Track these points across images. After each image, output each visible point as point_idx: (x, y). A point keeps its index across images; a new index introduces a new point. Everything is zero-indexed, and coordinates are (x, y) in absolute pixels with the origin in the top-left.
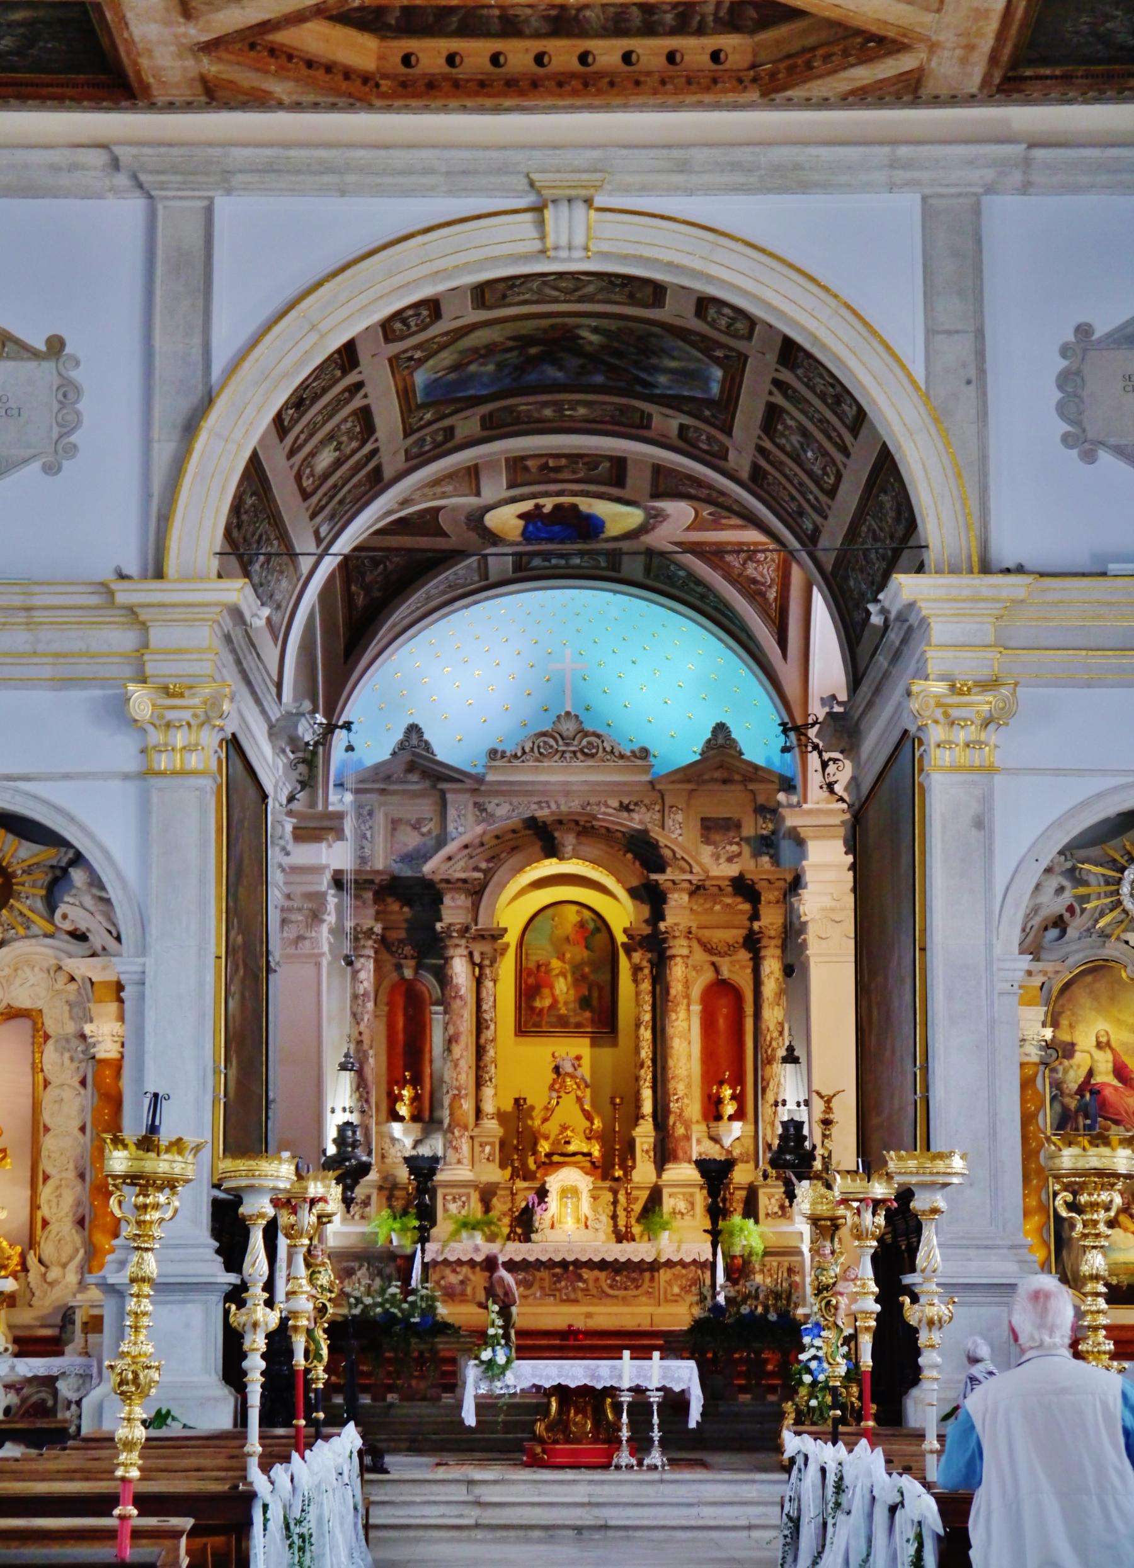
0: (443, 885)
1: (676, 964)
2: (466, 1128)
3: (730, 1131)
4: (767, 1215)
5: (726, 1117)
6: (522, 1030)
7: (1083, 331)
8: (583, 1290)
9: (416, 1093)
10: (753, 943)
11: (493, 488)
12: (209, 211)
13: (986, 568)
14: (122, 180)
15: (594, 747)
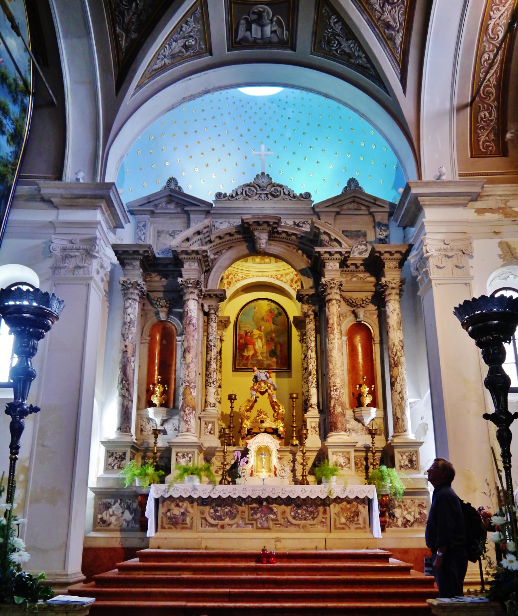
0: (184, 256)
1: (332, 305)
2: (194, 408)
3: (370, 413)
4: (401, 466)
5: (365, 405)
6: (236, 369)
8: (273, 520)
9: (165, 389)
15: (278, 192)
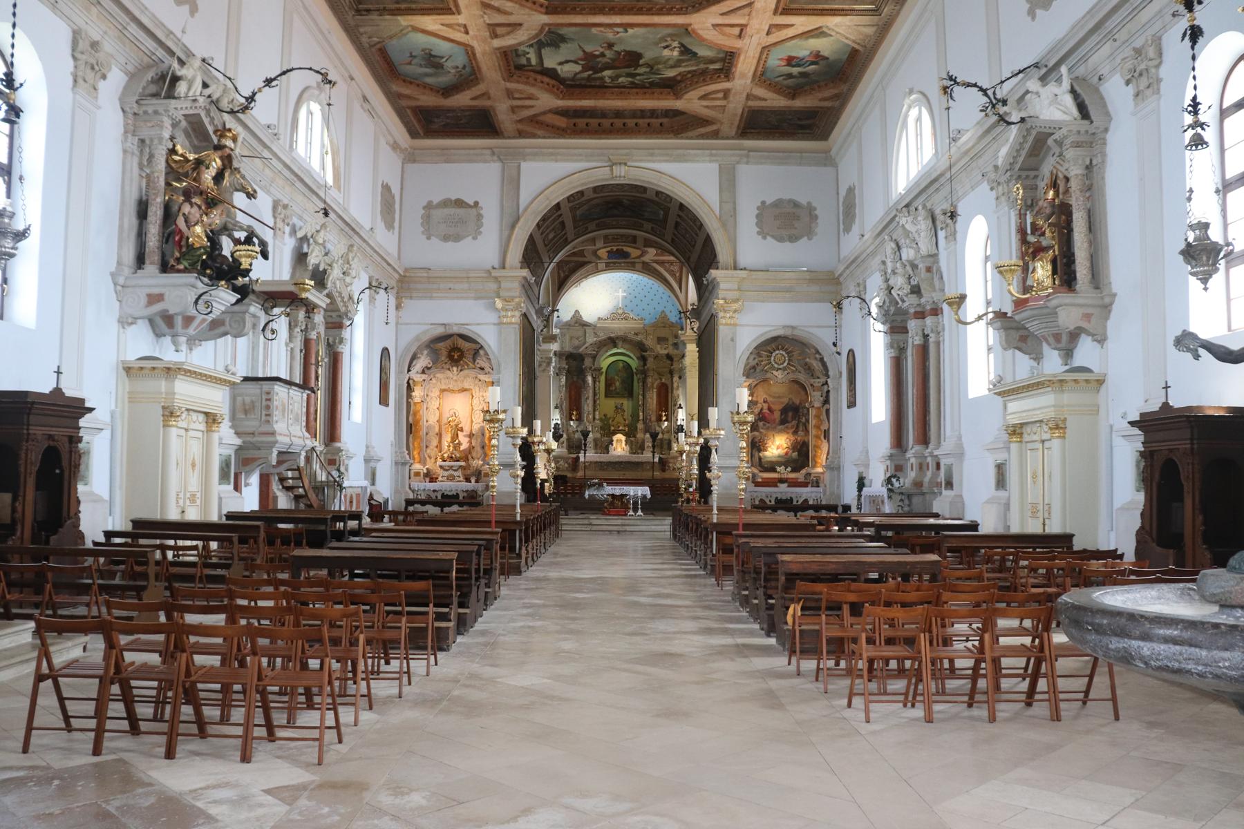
6: (606, 396)
7: (763, 203)
10: (671, 373)
11: (599, 244)
12: (519, 167)
13: (735, 268)
14: (495, 158)
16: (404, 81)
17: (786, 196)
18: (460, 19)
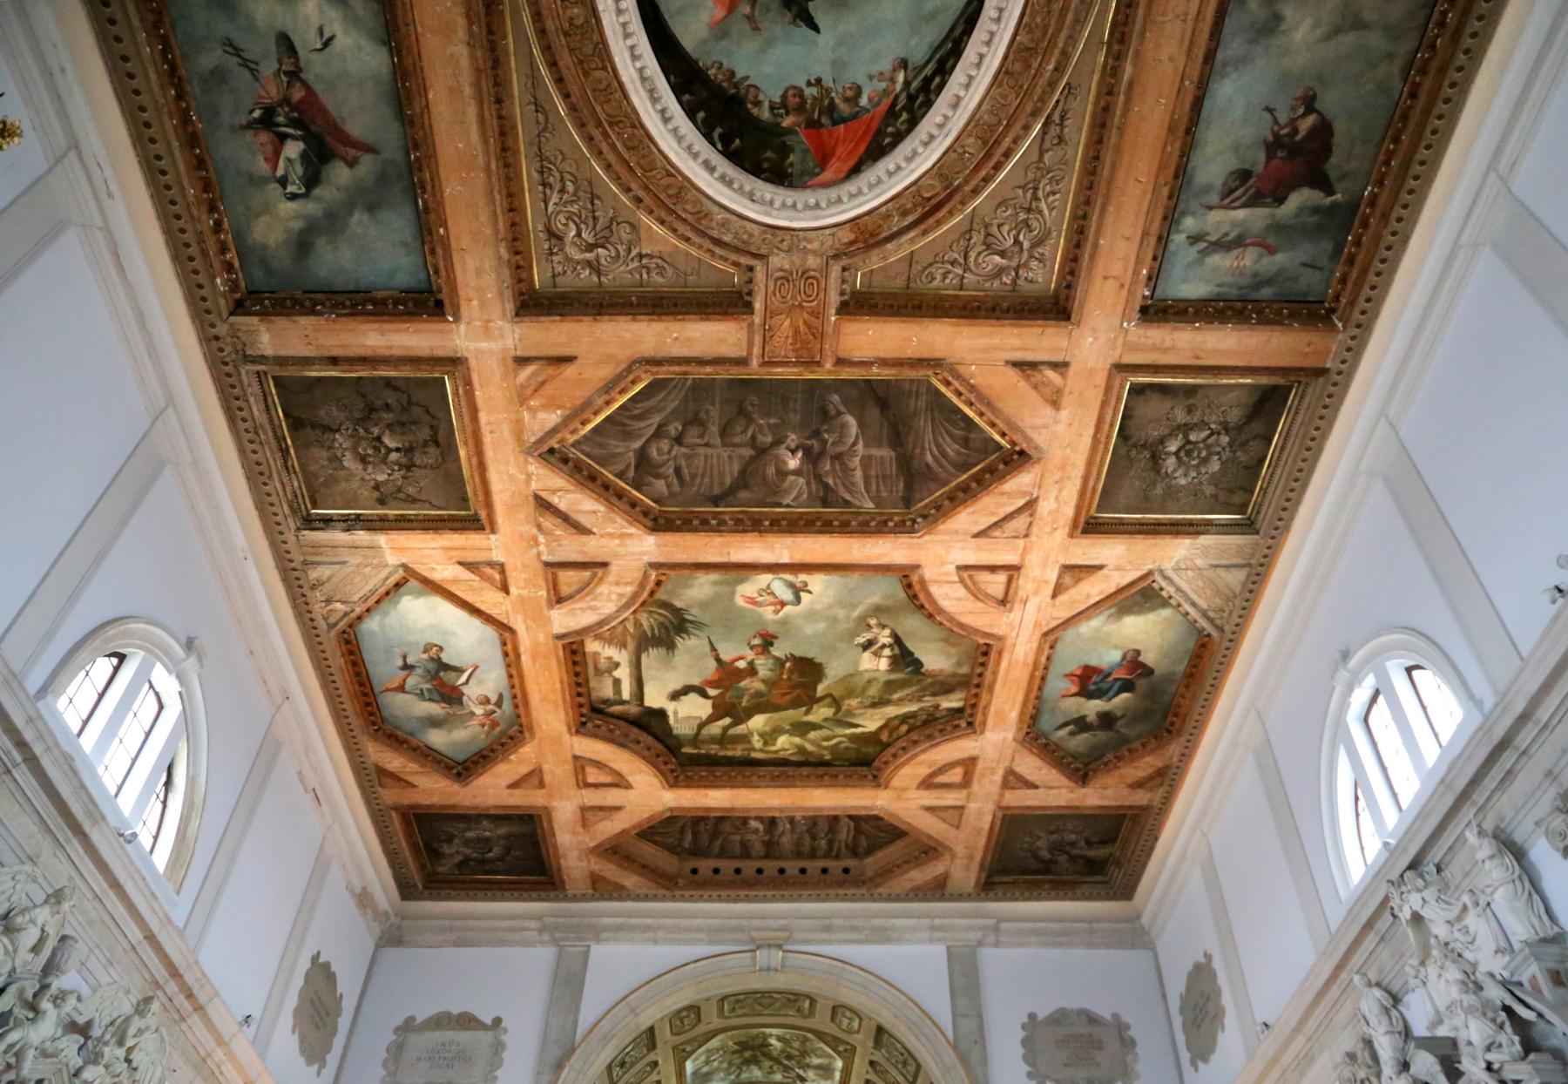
7: (1032, 1016)
12: (586, 955)
14: (546, 937)
16: (390, 736)
17: (1074, 1004)
18: (494, 546)
